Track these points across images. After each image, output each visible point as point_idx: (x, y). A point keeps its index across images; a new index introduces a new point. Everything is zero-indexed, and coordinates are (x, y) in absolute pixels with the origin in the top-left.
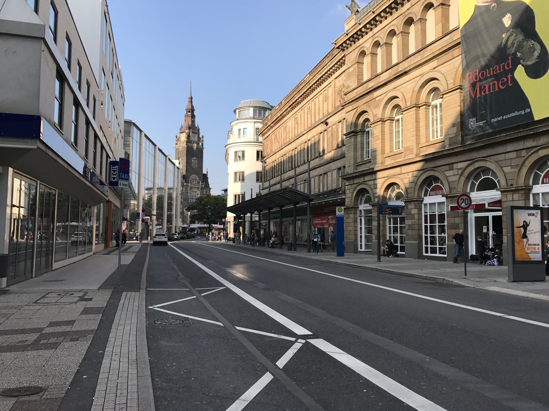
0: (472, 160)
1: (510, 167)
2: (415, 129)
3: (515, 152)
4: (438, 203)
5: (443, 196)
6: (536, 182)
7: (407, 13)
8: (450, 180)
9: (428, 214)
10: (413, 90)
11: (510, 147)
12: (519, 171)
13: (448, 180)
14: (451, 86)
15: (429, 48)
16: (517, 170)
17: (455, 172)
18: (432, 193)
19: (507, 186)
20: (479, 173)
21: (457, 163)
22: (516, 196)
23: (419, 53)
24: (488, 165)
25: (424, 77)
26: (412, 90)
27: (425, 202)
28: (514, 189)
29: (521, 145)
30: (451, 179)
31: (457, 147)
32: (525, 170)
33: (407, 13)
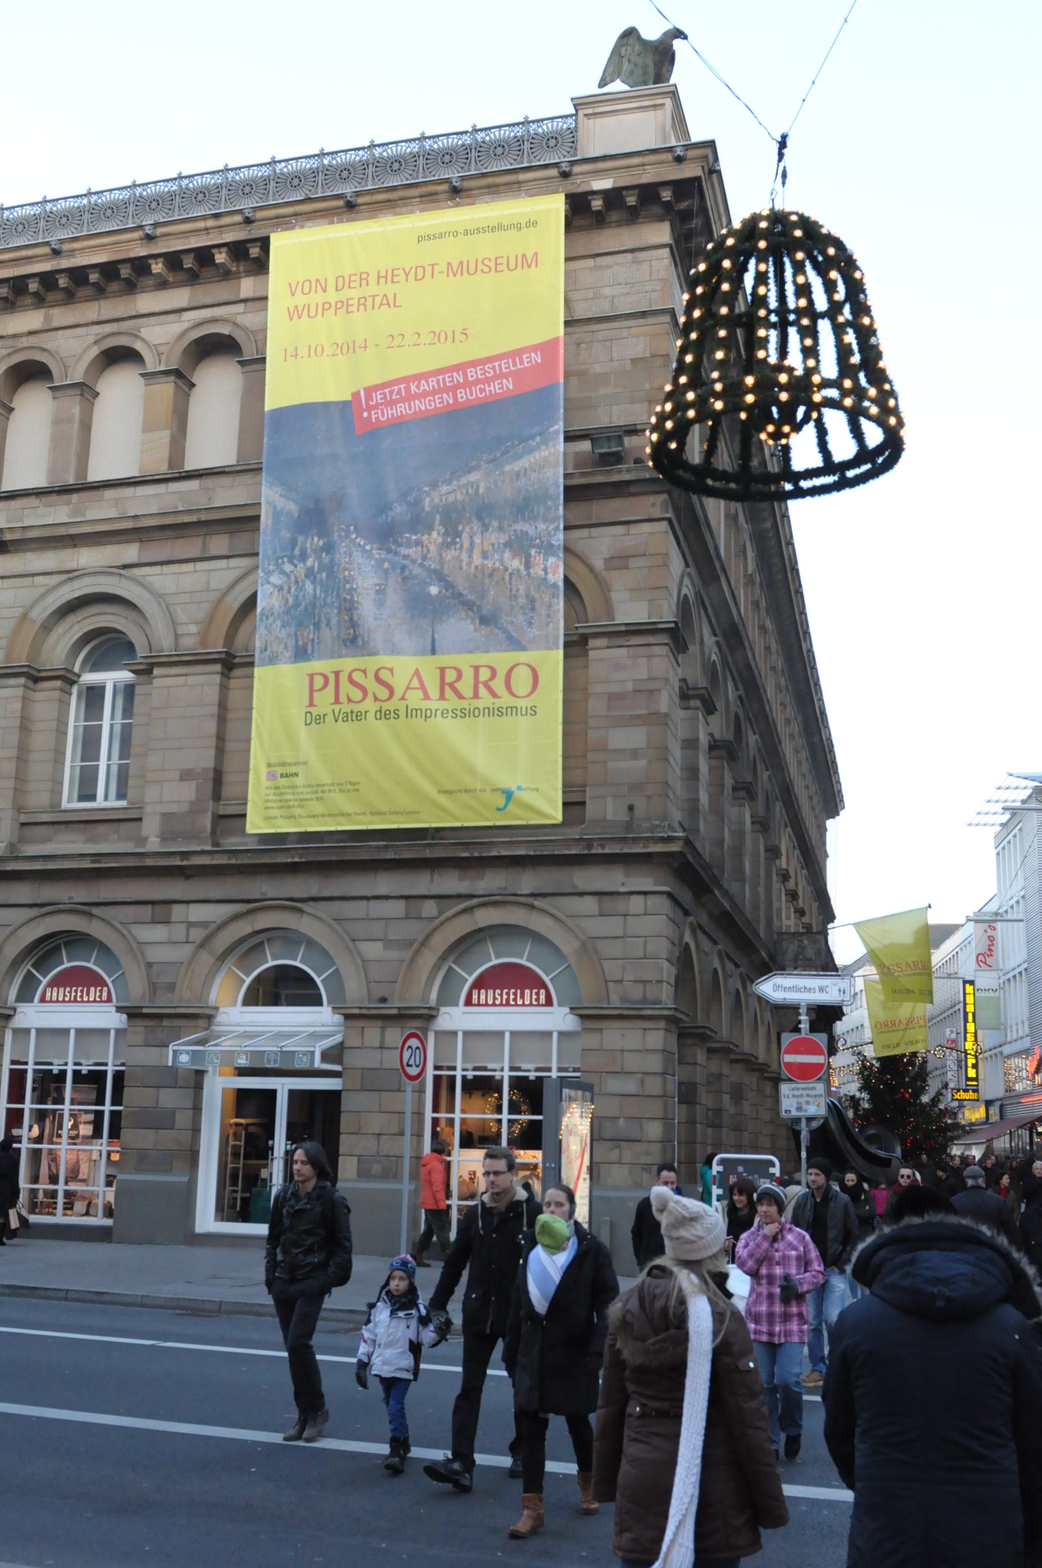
0: (249, 901)
1: (380, 944)
2: (14, 753)
3: (403, 902)
4: (80, 1032)
5: (119, 1009)
6: (447, 998)
7: (24, 342)
8: (151, 958)
9: (30, 1068)
10: (24, 616)
11: (385, 883)
12: (413, 960)
13: (143, 955)
14: (189, 643)
15: (109, 494)
16: (407, 955)
17: (179, 932)
18: (54, 993)
19: (370, 1000)
20: (261, 943)
21: (188, 902)
22: (394, 1035)
23: (65, 497)
24: (304, 925)
25: (77, 584)
26: (17, 612)
27: (20, 1021)
28: (395, 1012)
29: (421, 883)
30: (156, 955)
31: (203, 852)
32: (429, 959)
33: (24, 342)
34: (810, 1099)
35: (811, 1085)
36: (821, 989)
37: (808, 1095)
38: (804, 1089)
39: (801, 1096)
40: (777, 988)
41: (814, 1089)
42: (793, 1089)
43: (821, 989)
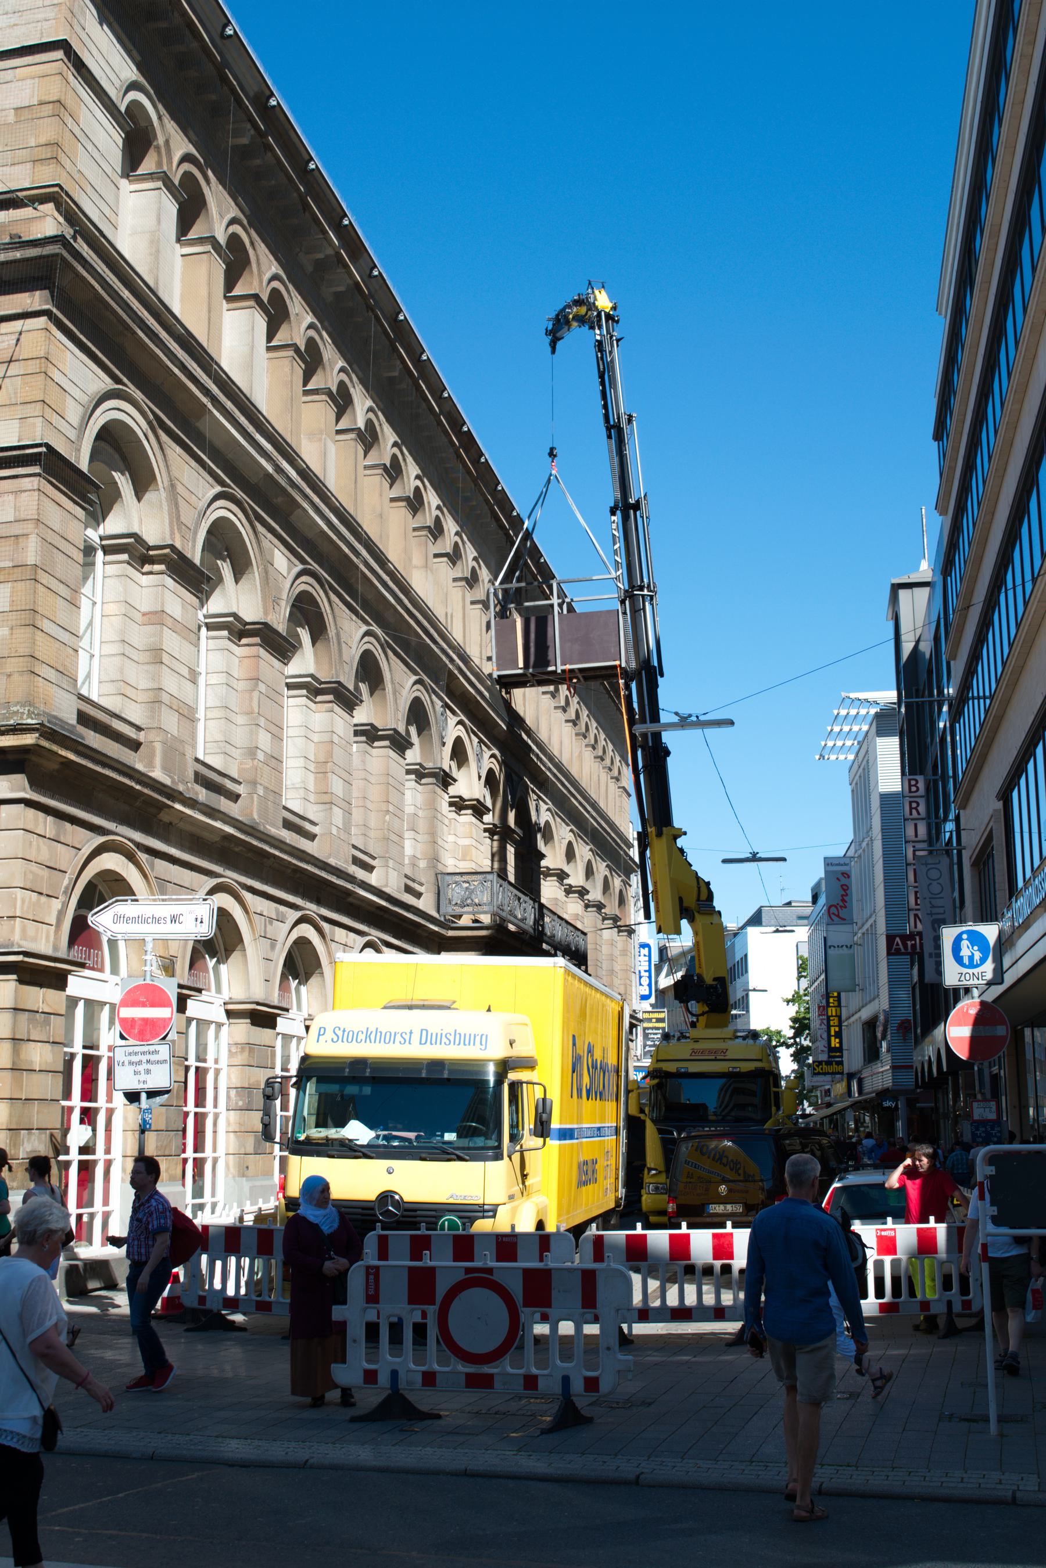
34: (149, 1066)
35: (152, 1048)
36: (174, 919)
37: (148, 1062)
38: (144, 1053)
39: (140, 1062)
40: (118, 919)
41: (157, 1052)
42: (130, 1054)
43: (174, 919)
